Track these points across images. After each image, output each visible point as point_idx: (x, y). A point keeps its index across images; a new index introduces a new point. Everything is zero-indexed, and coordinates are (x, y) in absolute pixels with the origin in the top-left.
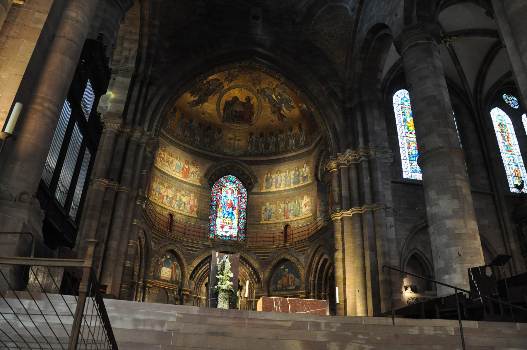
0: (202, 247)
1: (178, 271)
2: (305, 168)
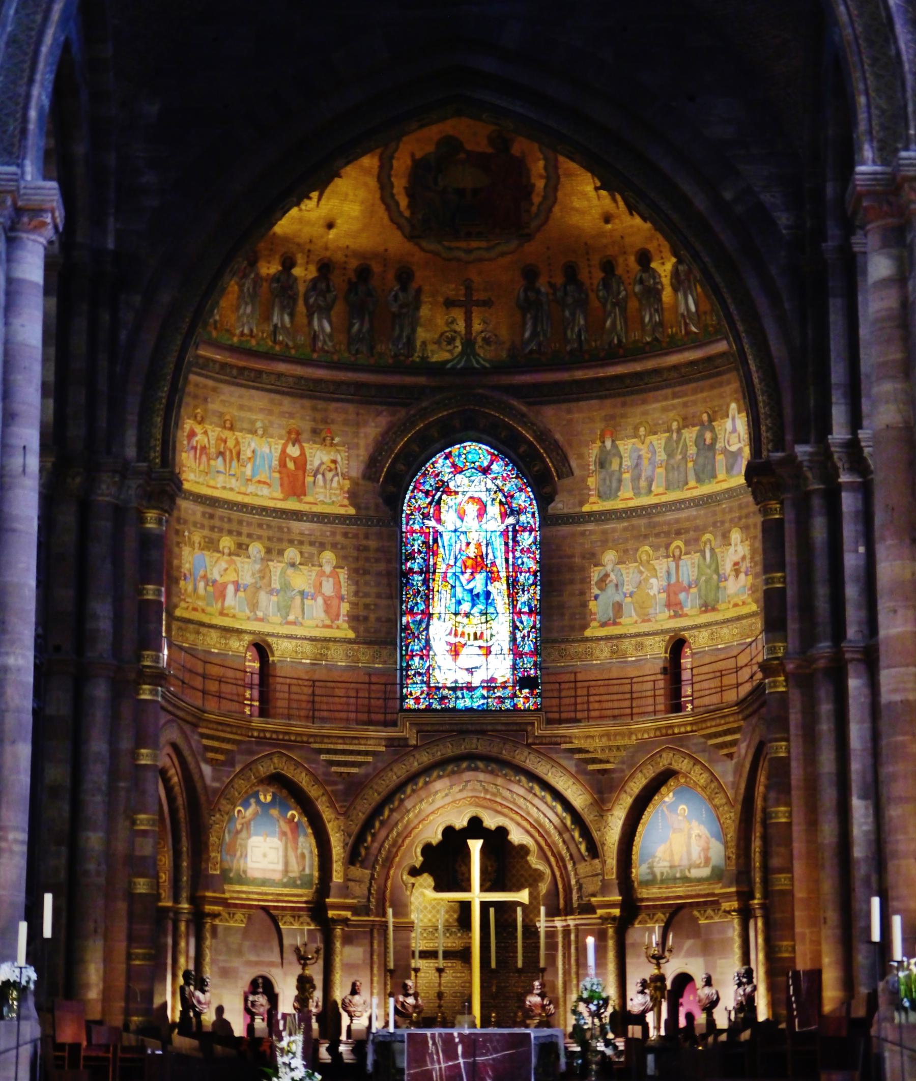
0: (383, 749)
1: (307, 843)
2: (733, 419)
